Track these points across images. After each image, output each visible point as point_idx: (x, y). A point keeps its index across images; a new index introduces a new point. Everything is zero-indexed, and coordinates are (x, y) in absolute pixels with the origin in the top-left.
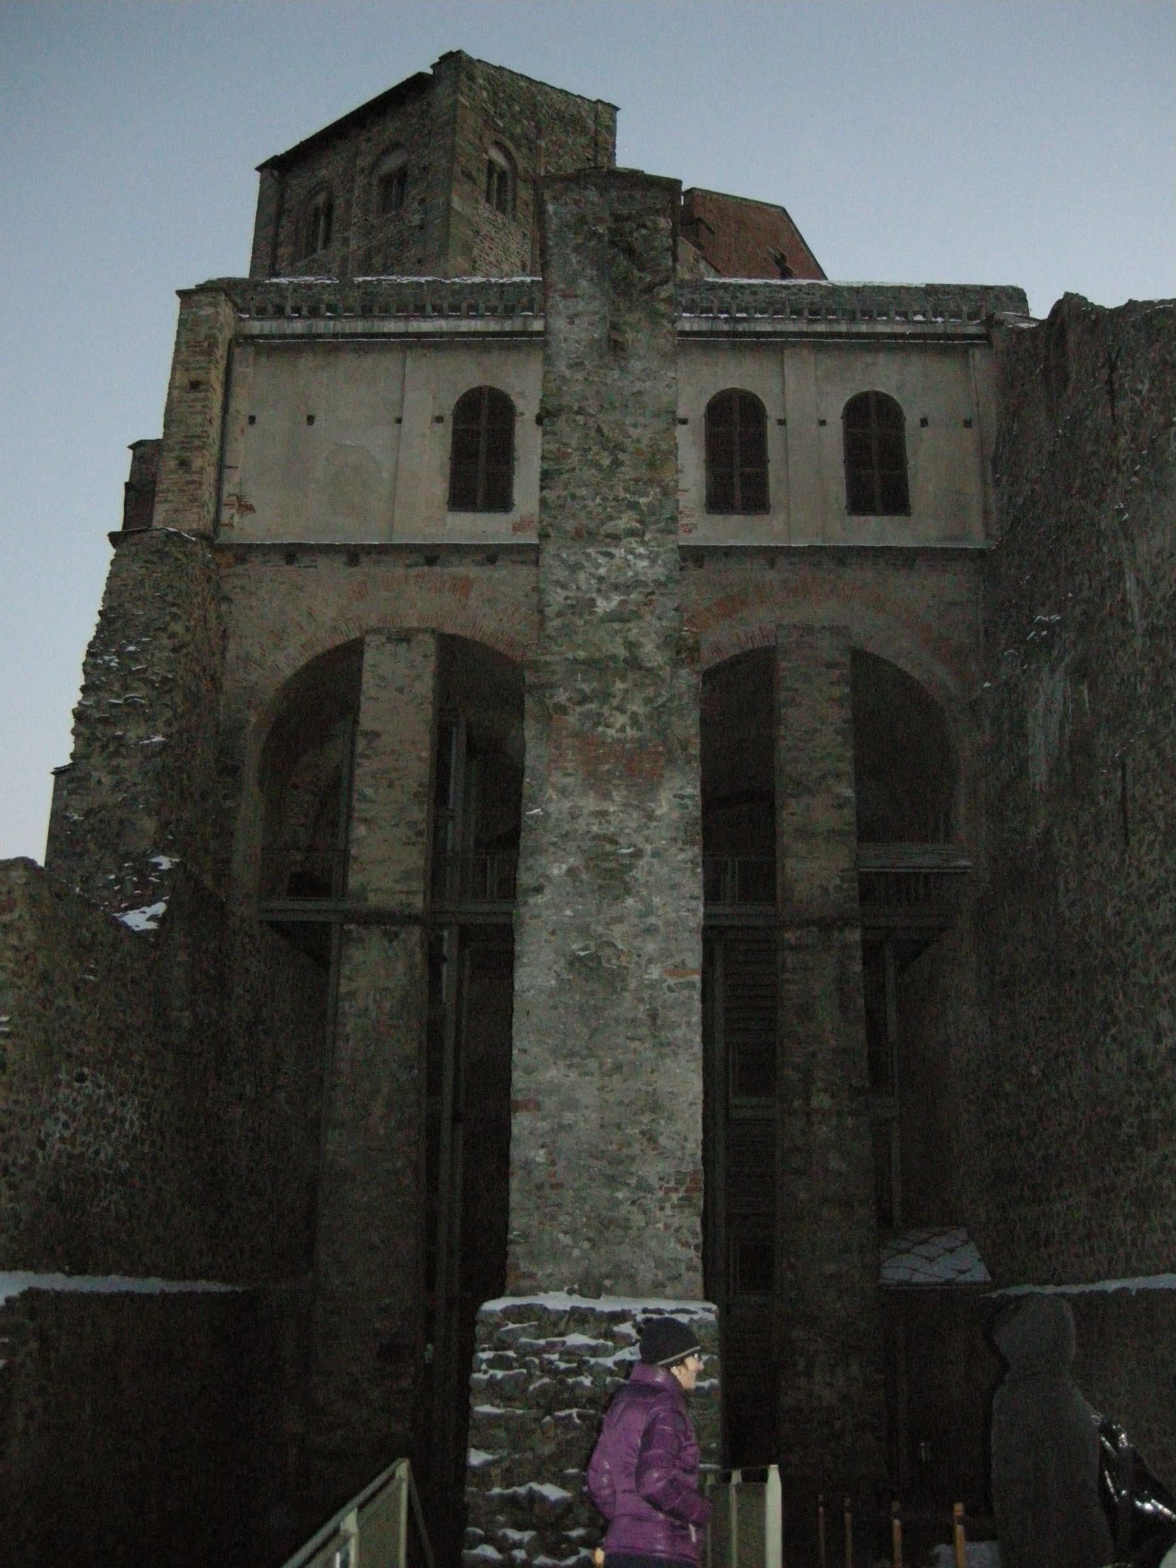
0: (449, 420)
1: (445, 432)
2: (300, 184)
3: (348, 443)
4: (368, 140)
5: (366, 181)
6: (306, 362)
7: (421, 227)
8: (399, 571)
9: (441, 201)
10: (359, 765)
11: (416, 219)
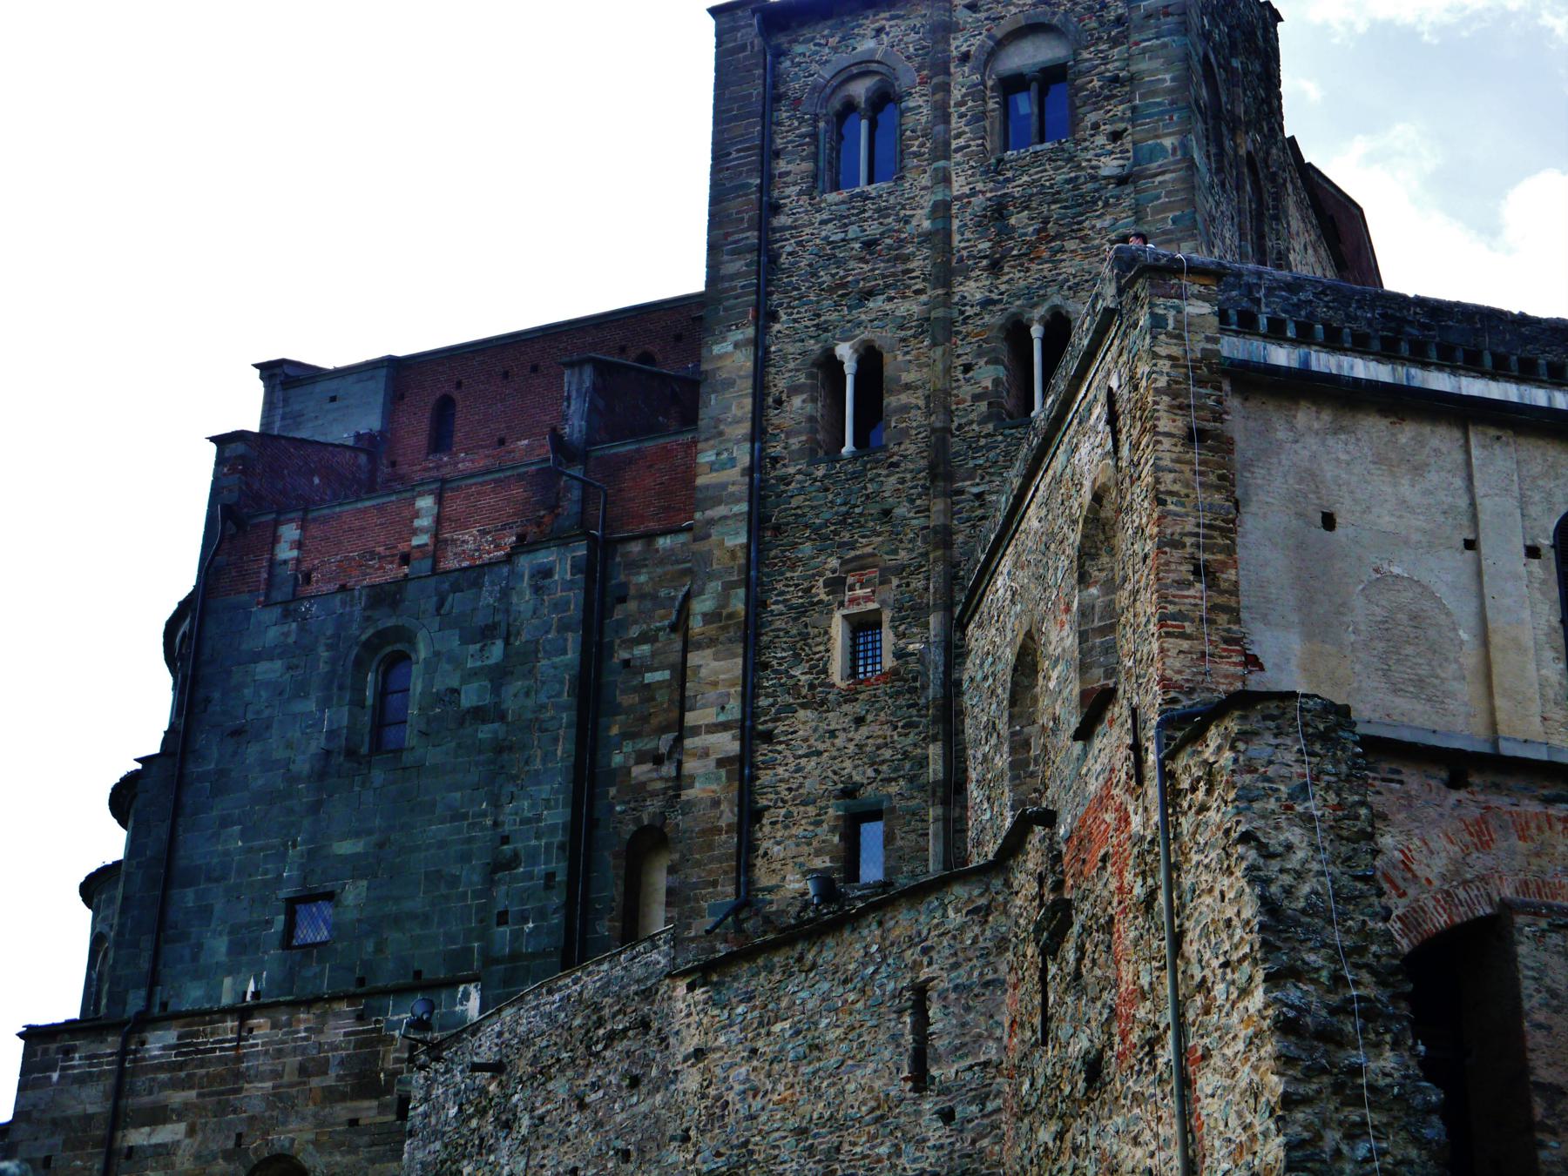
0: (1549, 555)
1: (1544, 571)
3: (1396, 570)
5: (976, 78)
6: (1305, 417)
7: (1121, 181)
8: (1532, 807)
9: (1168, 142)
10: (1542, 1145)
11: (1110, 166)
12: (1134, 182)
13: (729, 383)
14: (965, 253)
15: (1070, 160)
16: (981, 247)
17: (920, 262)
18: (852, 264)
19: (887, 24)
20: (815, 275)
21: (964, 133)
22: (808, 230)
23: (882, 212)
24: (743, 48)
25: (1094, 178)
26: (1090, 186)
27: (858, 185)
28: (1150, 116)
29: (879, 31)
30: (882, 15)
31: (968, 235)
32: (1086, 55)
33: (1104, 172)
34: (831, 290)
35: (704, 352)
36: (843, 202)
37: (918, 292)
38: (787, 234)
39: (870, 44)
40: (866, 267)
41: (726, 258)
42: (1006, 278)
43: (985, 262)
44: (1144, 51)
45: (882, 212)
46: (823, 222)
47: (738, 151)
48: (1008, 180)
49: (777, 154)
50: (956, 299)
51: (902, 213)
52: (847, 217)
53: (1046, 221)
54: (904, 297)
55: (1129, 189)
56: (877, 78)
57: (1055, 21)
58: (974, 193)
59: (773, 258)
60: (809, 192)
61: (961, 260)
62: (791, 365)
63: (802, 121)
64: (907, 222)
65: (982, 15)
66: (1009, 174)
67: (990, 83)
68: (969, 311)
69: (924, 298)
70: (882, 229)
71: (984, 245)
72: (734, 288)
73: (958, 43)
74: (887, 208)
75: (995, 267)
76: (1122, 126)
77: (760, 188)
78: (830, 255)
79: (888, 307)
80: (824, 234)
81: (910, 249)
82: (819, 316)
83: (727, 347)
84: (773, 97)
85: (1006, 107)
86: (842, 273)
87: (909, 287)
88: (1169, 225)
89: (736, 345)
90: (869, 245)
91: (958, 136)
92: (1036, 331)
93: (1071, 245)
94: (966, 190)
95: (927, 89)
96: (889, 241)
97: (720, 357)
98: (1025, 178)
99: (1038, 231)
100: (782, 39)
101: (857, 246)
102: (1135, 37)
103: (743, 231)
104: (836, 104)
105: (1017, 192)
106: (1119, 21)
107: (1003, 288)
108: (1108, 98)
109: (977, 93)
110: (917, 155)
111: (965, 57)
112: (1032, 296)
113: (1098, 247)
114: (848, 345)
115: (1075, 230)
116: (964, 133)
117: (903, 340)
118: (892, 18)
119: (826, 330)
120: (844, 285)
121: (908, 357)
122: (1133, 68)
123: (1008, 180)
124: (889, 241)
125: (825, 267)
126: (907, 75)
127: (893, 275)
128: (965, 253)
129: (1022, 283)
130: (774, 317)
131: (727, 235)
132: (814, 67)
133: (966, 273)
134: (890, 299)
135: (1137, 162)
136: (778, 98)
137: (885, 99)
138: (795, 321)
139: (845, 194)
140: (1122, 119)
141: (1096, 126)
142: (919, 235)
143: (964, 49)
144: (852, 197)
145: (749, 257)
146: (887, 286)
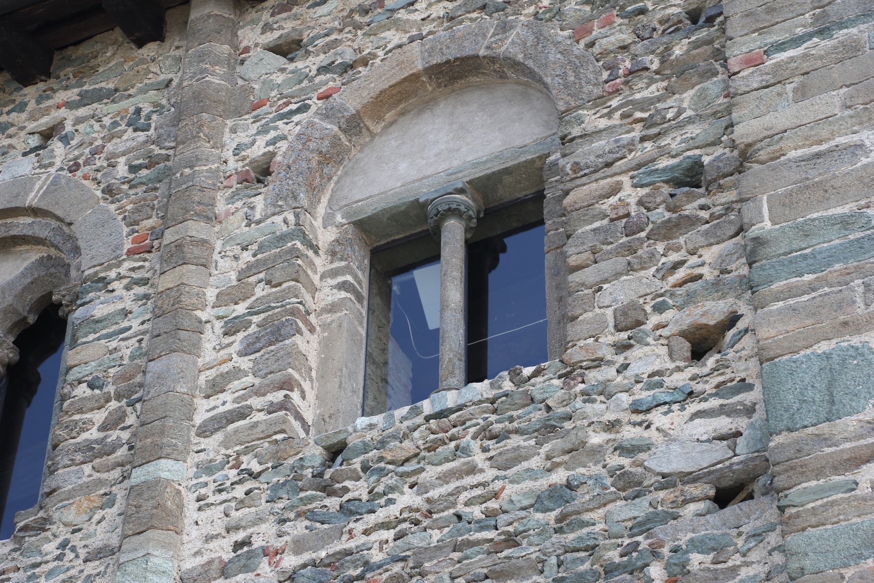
4: (287, 49)
11: (686, 440)
12: (770, 490)
15: (548, 429)
21: (237, 373)
25: (629, 485)
26: (624, 511)
30: (62, 96)
33: (667, 459)
39: (26, 166)
56: (34, 255)
65: (309, 64)
66: (359, 489)
73: (243, 137)
76: (712, 310)
91: (216, 388)
94: (222, 549)
98: (407, 498)
108: (666, 232)
116: (237, 373)
118: (85, 100)
123: (349, 511)
140: (717, 287)
141: (630, 322)
143: (258, 150)
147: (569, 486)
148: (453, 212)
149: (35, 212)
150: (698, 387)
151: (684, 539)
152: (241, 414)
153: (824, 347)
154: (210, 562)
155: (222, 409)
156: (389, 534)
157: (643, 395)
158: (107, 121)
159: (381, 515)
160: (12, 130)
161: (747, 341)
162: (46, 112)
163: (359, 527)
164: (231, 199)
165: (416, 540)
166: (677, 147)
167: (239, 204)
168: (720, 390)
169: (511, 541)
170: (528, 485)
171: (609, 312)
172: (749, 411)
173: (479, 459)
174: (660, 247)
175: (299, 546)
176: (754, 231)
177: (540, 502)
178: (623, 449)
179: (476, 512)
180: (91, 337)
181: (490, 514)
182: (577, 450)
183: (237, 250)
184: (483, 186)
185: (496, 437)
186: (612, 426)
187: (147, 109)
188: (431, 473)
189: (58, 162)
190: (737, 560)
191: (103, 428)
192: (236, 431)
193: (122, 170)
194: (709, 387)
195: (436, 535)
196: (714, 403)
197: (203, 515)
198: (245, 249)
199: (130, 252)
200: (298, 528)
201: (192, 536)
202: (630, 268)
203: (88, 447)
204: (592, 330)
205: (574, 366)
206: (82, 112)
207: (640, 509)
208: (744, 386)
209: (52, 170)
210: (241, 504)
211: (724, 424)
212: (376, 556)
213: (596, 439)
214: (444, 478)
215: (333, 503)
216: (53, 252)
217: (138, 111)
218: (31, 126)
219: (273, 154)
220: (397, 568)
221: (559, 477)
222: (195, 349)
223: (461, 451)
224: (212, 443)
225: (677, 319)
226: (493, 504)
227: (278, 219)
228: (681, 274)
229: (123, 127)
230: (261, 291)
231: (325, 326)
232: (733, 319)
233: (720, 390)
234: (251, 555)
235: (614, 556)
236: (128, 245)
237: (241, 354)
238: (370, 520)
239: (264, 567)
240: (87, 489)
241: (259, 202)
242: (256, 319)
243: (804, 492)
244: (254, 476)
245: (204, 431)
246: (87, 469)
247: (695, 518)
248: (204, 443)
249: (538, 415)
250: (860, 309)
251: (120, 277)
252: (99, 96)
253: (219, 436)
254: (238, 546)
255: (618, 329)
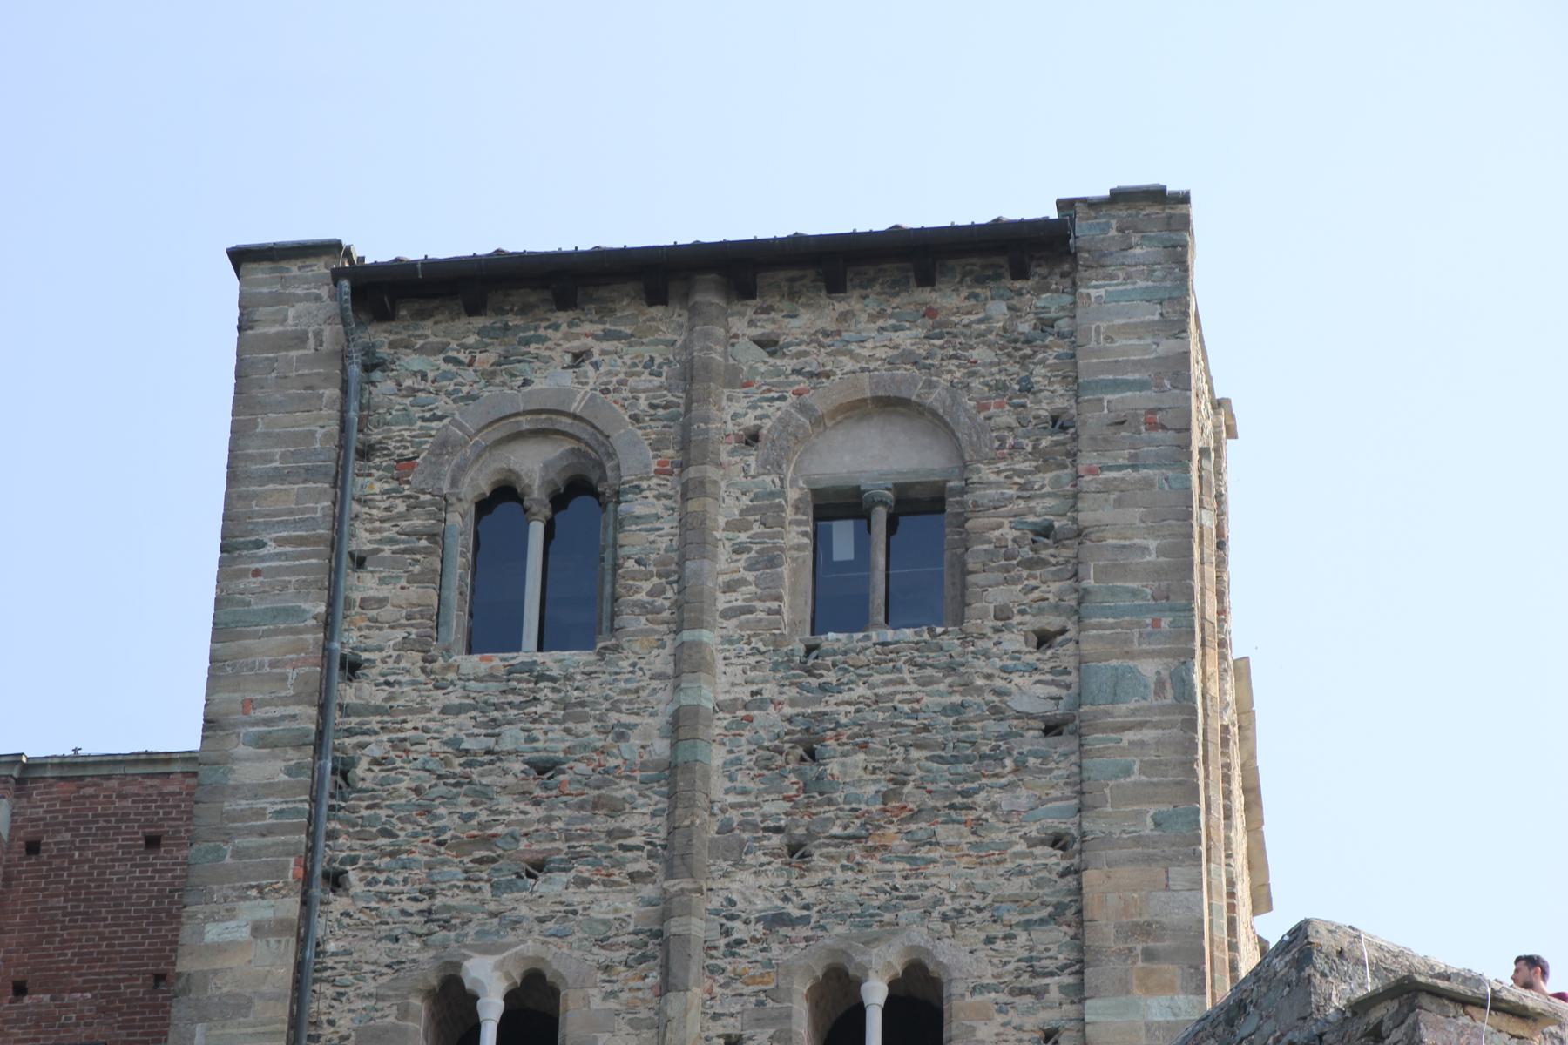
2: (436, 377)
4: (769, 344)
5: (769, 481)
7: (1052, 729)
9: (1149, 669)
11: (1032, 694)
12: (1078, 734)
13: (238, 1006)
14: (735, 816)
15: (951, 669)
16: (768, 808)
17: (643, 819)
18: (504, 802)
19: (597, 347)
20: (427, 811)
22: (415, 720)
23: (572, 710)
24: (300, 339)
25: (997, 712)
26: (994, 727)
27: (516, 646)
28: (1116, 612)
29: (579, 358)
30: (587, 327)
31: (742, 780)
32: (986, 473)
33: (1024, 705)
34: (460, 846)
35: (185, 934)
36: (492, 677)
37: (633, 876)
38: (374, 722)
39: (568, 379)
40: (535, 813)
41: (243, 750)
42: (817, 878)
43: (776, 840)
44: (1106, 488)
45: (572, 710)
46: (445, 710)
47: (280, 542)
48: (824, 688)
49: (360, 562)
50: (716, 902)
51: (614, 717)
52: (497, 707)
53: (899, 780)
54: (608, 883)
55: (1065, 744)
56: (568, 445)
57: (933, 399)
58: (758, 700)
59: (343, 770)
60: (422, 646)
61: (726, 828)
62: (369, 986)
63: (414, 504)
64: (621, 737)
65: (787, 364)
66: (831, 677)
67: (793, 494)
68: (740, 930)
69: (649, 890)
70: (570, 741)
71: (775, 807)
72: (260, 814)
73: (737, 407)
74: (582, 704)
75: (797, 851)
76: (1052, 622)
77: (328, 624)
78: (461, 772)
79: (577, 897)
80: (449, 732)
81: (624, 790)
82: (432, 894)
83: (236, 930)
84: (355, 448)
85: (820, 542)
86: (484, 816)
87: (619, 864)
88: (1148, 827)
89: (257, 930)
90: (544, 768)
91: (730, 587)
92: (875, 994)
93: (945, 833)
94: (744, 693)
95: (671, 485)
96: (581, 767)
97: (220, 949)
98: (861, 690)
99: (886, 797)
100: (379, 336)
101: (518, 767)
102: (1088, 459)
103: (285, 701)
104: (480, 482)
105: (844, 714)
106: (1057, 422)
107: (810, 895)
108: (1030, 564)
109: (766, 509)
110: (646, 609)
111: (752, 438)
112: (870, 922)
113: (1005, 846)
114: (490, 960)
115: (958, 804)
117: (607, 969)
118: (608, 336)
119: (445, 925)
120: (488, 841)
121: (612, 1004)
122: (1085, 517)
123: (824, 688)
124: (581, 767)
125: (449, 800)
126: (637, 457)
127: (588, 835)
128: (735, 816)
129: (848, 894)
130: (336, 881)
131: (248, 705)
132: (443, 404)
133: (736, 855)
134: (583, 883)
135: (1079, 701)
136: (366, 453)
137: (581, 490)
138: (383, 898)
139: (497, 661)
140: (1056, 609)
141: (1003, 614)
142: (644, 766)
143: (749, 421)
144: (512, 670)
145: (294, 756)
146: (576, 856)
147: (962, 705)
148: (883, 503)
149: (575, 417)
150: (1041, 666)
151: (1026, 749)
152: (750, 611)
153: (1114, 663)
154: (736, 699)
155: (735, 604)
156: (851, 709)
157: (1009, 663)
158: (627, 359)
159: (846, 696)
160: (549, 344)
161: (1071, 646)
162: (577, 337)
163: (832, 700)
164: (732, 453)
165: (869, 716)
166: (1042, 508)
167: (738, 459)
168: (1053, 671)
169: (926, 729)
170: (937, 699)
171: (991, 607)
172: (1068, 687)
173: (907, 676)
174: (1025, 573)
175: (793, 703)
176: (1084, 584)
177: (944, 711)
178: (995, 692)
179: (906, 708)
180: (634, 528)
181: (914, 711)
182: (967, 686)
183: (739, 494)
184: (900, 489)
185: (921, 666)
186: (989, 677)
187: (658, 360)
188: (877, 678)
189: (591, 382)
190: (1052, 765)
191: (650, 594)
192: (747, 621)
193: (643, 404)
194: (1047, 667)
195: (881, 716)
196: (1049, 677)
197: (728, 669)
198: (744, 494)
199: (656, 471)
200: (793, 692)
201: (723, 682)
202: (1006, 581)
203: (642, 605)
204: (980, 617)
205: (971, 635)
206: (606, 345)
207: (1003, 727)
208: (1066, 672)
209: (588, 388)
210: (753, 668)
211: (1054, 691)
212: (844, 720)
213: (980, 682)
214: (886, 683)
215: (814, 682)
216: (583, 447)
217: (652, 359)
218: (567, 345)
219: (760, 427)
220: (856, 729)
221: (957, 699)
222: (714, 558)
223: (900, 670)
224: (731, 624)
225: (1034, 622)
226: (916, 706)
227: (768, 479)
228: (1036, 594)
229: (639, 369)
230: (757, 528)
231: (794, 560)
232: (1063, 631)
233: (1053, 671)
234: (762, 701)
235: (986, 750)
236: (654, 467)
237: (748, 569)
238: (840, 697)
239: (771, 708)
240: (646, 633)
241: (752, 460)
242: (755, 547)
243: (1095, 739)
244: (762, 653)
245: (726, 614)
246: (643, 619)
247: (1032, 738)
248: (725, 623)
249: (944, 659)
250: (1136, 646)
251: (650, 488)
252: (618, 336)
253: (735, 622)
254: (753, 694)
255: (996, 618)
